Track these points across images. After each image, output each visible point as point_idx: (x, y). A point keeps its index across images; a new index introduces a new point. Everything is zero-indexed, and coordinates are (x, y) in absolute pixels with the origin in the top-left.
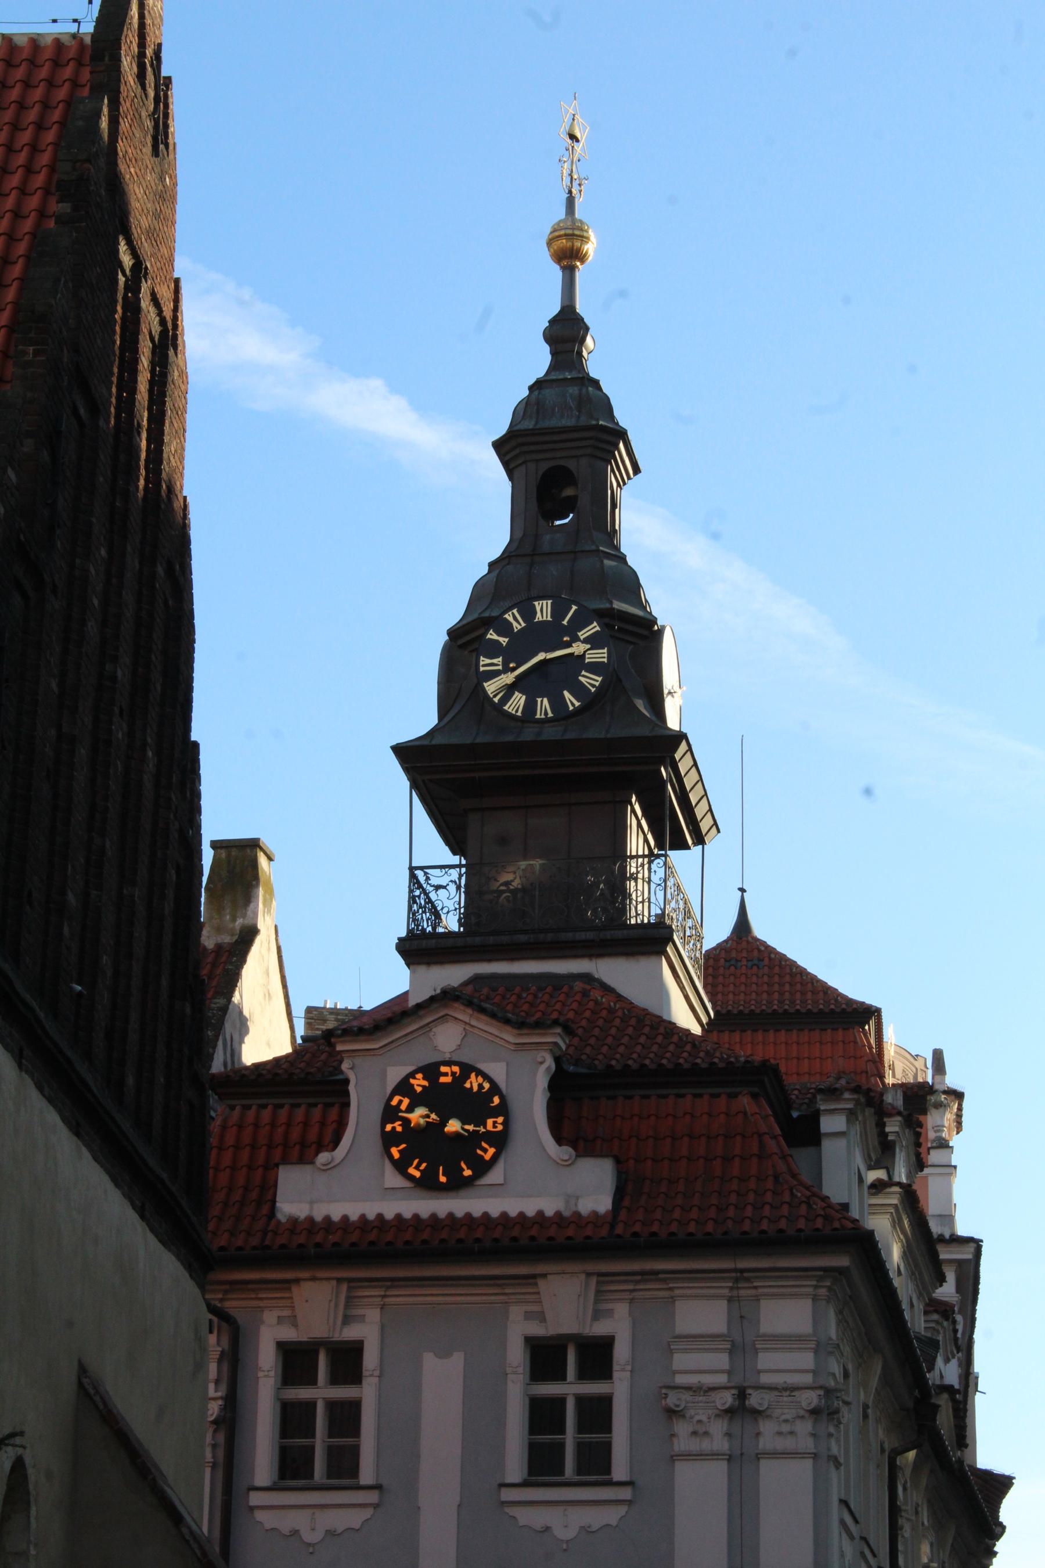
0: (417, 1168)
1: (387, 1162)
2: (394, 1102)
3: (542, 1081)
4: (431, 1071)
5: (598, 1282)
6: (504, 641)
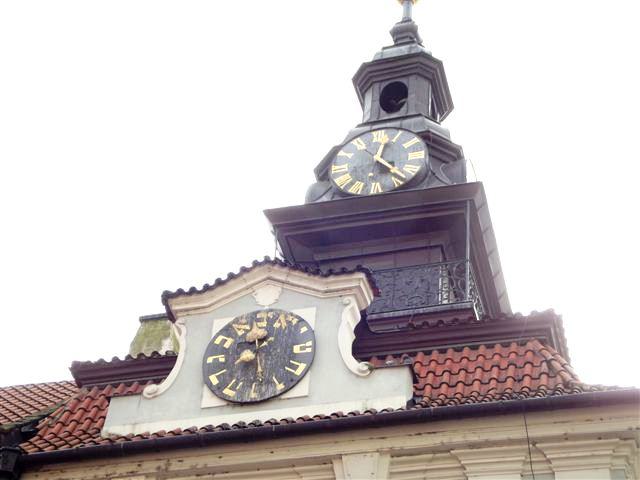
0: (232, 388)
1: (206, 388)
2: (217, 342)
3: (350, 319)
4: (253, 318)
5: (392, 464)
6: (350, 155)
